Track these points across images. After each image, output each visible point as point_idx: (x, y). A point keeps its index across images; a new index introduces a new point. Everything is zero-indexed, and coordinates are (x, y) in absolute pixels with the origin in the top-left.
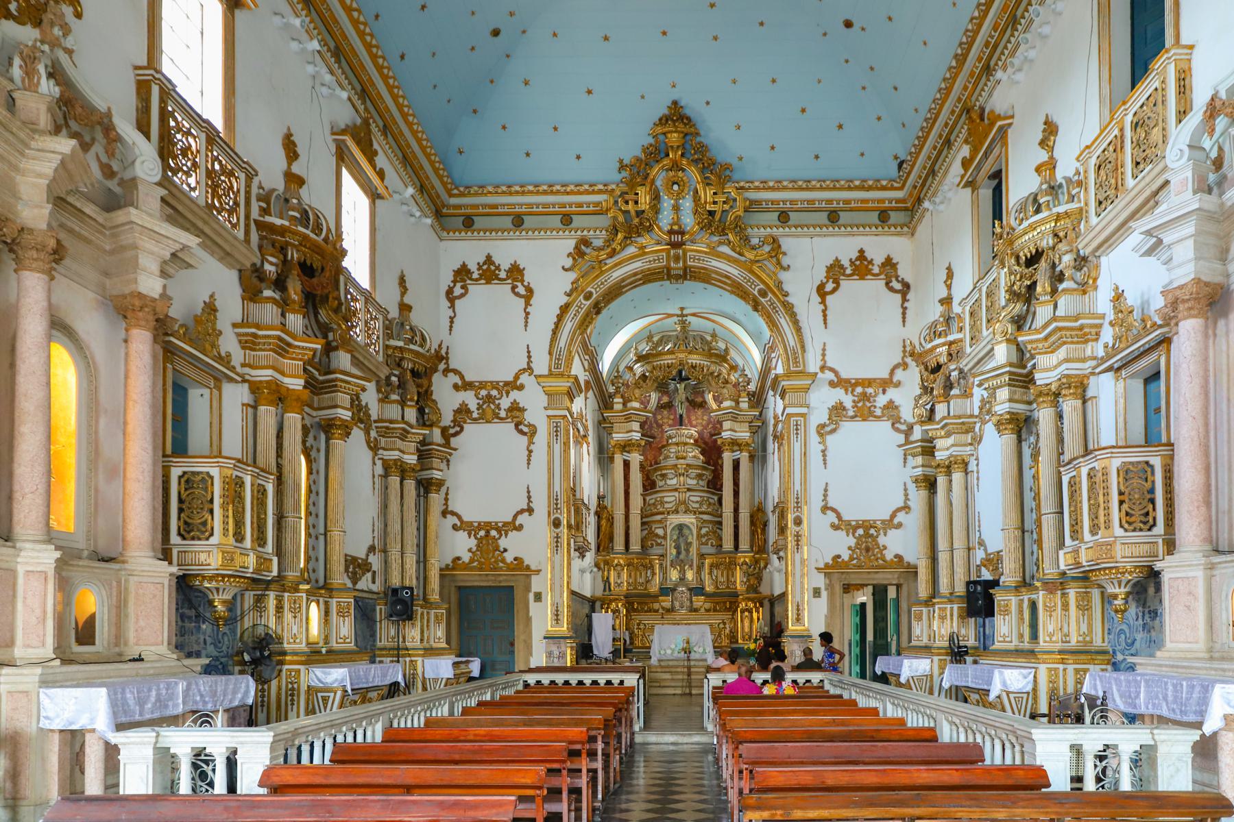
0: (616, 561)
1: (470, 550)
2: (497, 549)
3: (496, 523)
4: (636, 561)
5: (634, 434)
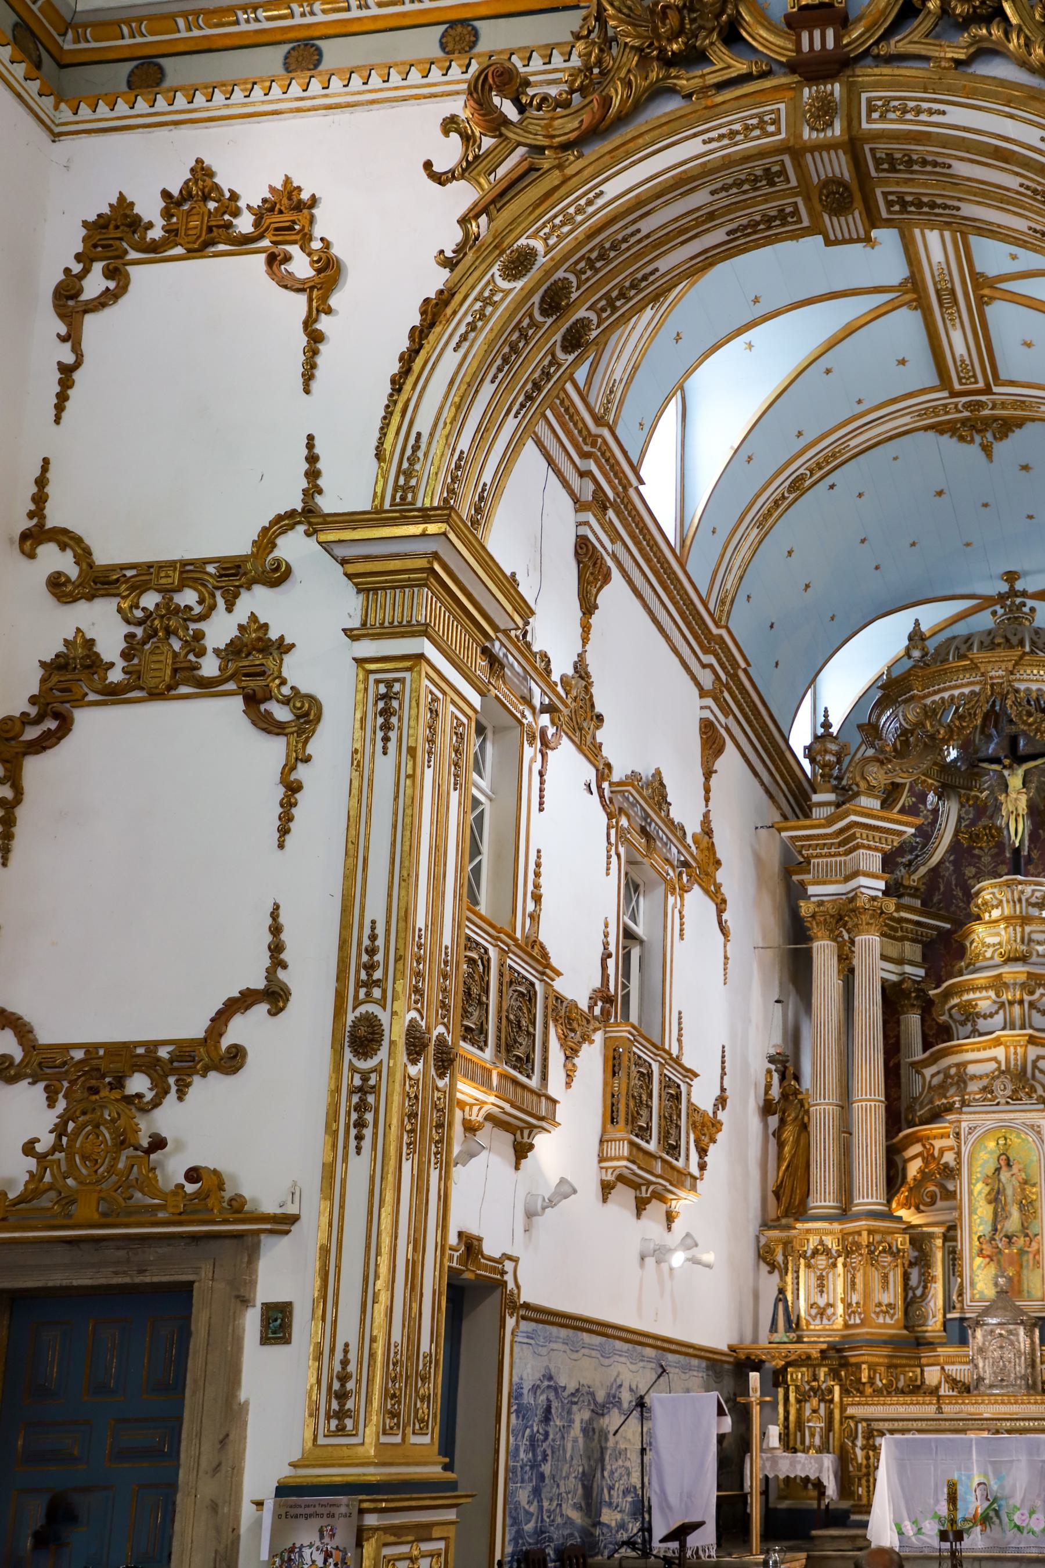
0: (813, 1242)
1: (29, 1148)
2: (124, 1140)
3: (152, 1046)
4: (864, 1239)
5: (863, 881)
